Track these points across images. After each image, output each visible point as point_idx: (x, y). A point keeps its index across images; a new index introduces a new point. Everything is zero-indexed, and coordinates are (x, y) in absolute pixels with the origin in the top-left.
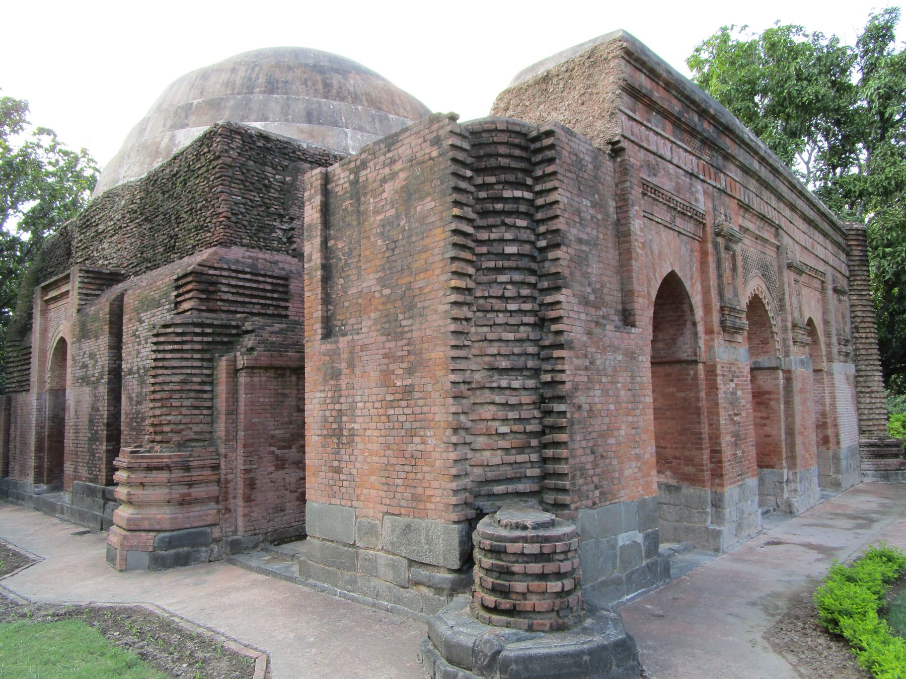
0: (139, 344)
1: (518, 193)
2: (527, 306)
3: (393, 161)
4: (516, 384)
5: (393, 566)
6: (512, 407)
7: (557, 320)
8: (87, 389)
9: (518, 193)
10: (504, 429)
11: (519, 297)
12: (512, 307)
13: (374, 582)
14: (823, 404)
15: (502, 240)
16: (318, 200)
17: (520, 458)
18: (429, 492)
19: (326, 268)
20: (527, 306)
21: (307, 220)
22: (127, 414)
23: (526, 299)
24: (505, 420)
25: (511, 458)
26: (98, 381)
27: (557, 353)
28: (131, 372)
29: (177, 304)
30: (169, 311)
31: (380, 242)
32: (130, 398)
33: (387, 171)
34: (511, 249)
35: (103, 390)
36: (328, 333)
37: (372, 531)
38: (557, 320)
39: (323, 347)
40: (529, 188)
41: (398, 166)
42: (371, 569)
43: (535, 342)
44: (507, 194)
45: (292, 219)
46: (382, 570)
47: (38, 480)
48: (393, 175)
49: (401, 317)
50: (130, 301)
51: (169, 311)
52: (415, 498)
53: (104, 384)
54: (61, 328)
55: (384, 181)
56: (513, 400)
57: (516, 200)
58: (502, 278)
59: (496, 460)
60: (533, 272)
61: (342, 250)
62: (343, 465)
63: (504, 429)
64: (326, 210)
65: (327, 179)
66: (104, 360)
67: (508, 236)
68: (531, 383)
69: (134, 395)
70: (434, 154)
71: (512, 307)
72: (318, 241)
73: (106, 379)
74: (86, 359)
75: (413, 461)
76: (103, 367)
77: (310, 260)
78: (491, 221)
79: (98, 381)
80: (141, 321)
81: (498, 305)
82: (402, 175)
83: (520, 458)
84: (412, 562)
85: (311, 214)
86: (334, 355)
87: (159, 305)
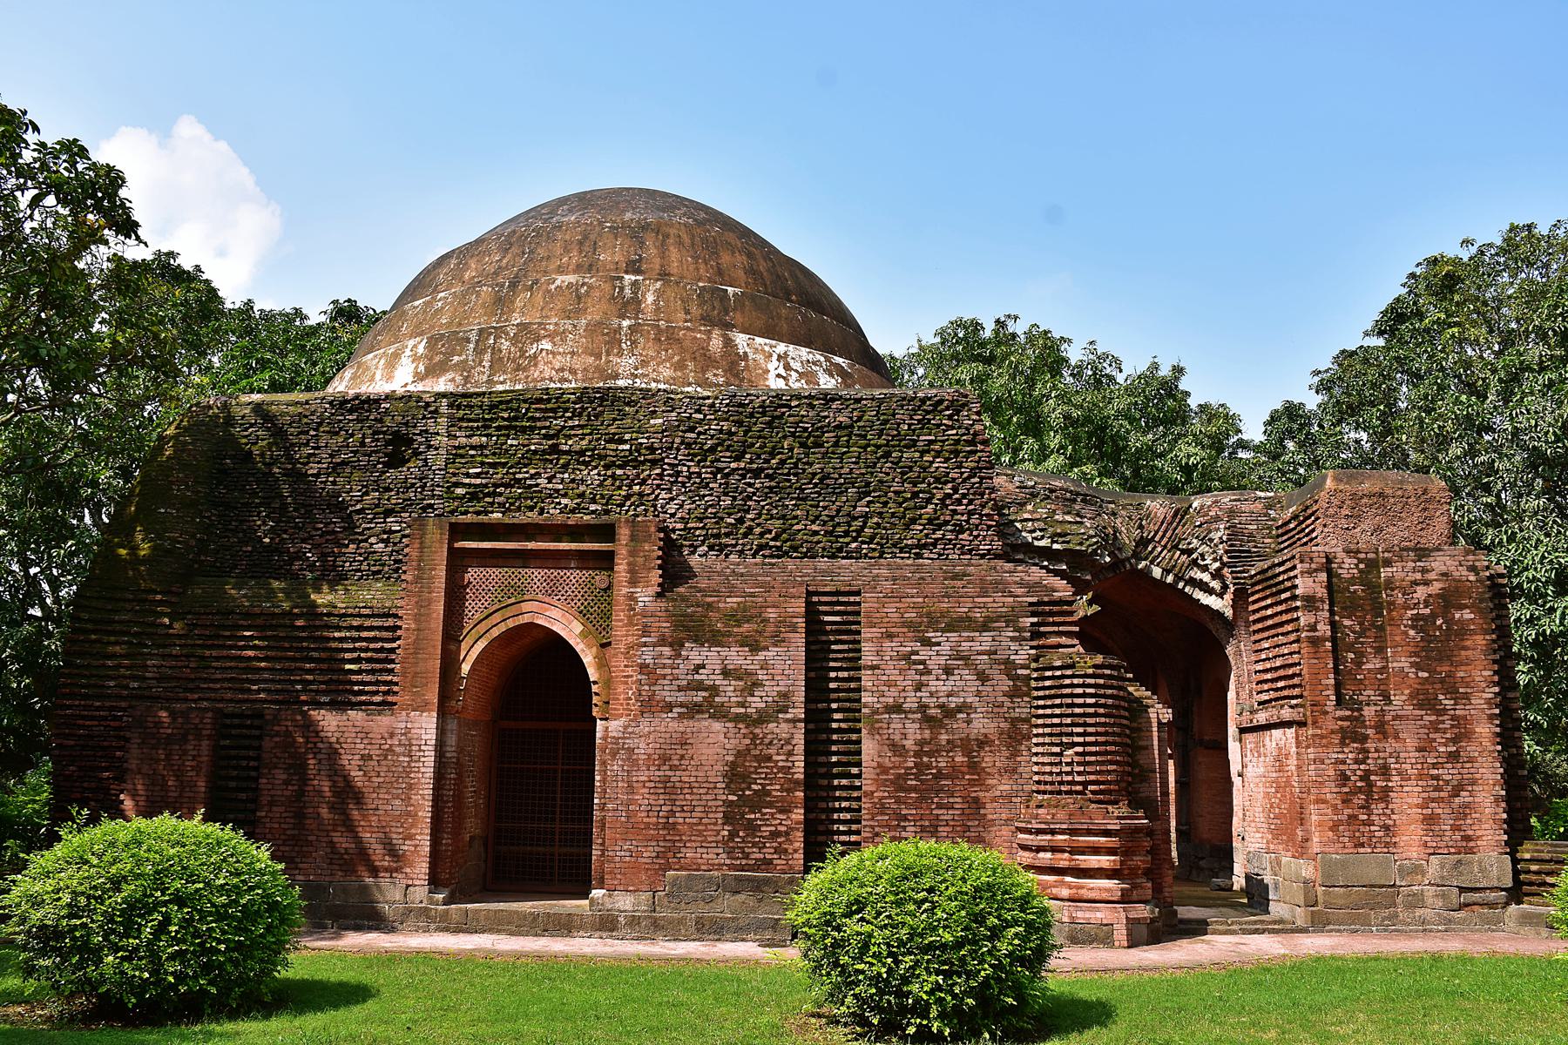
5: (1443, 896)
8: (717, 726)
13: (1419, 912)
16: (1323, 576)
18: (1479, 833)
22: (883, 769)
28: (897, 708)
31: (1412, 633)
33: (1418, 576)
35: (790, 733)
37: (1417, 870)
39: (1339, 713)
41: (1432, 576)
42: (1416, 901)
46: (1430, 901)
47: (435, 882)
48: (1427, 583)
49: (1441, 697)
52: (1467, 838)
53: (794, 721)
61: (1349, 628)
62: (1373, 817)
64: (1330, 587)
69: (909, 743)
70: (1472, 578)
72: (1327, 614)
75: (1464, 812)
76: (785, 695)
84: (1462, 890)
87: (984, 627)
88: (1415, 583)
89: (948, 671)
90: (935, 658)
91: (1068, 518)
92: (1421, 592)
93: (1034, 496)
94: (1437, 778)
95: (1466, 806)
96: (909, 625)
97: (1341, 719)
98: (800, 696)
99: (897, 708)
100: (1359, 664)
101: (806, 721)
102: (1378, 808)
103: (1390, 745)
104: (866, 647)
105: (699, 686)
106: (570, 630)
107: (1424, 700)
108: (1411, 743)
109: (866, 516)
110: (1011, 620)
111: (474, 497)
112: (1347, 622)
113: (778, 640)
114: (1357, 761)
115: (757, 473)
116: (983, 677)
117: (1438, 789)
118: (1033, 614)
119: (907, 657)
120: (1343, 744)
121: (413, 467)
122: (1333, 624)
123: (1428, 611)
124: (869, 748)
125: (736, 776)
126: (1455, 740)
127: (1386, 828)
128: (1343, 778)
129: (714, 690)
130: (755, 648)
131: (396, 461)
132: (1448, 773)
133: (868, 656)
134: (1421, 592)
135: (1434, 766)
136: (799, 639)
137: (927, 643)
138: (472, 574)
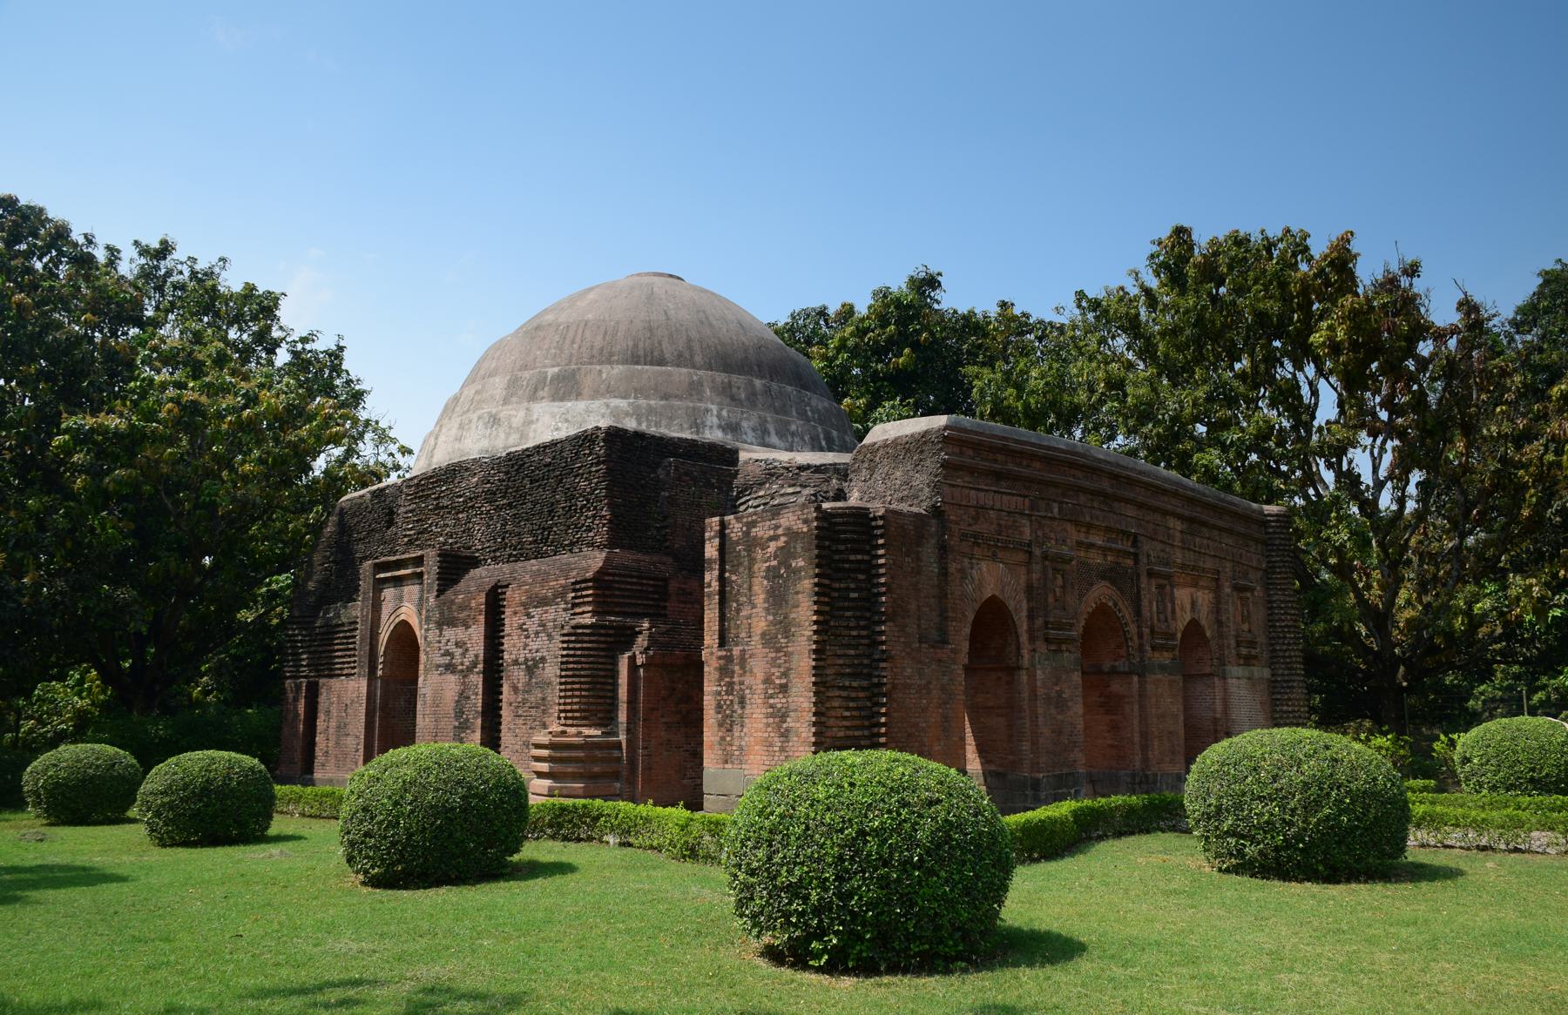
0: (527, 637)
1: (859, 557)
2: (864, 633)
3: (777, 527)
4: (855, 684)
6: (853, 700)
7: (883, 643)
8: (452, 678)
9: (859, 557)
10: (847, 714)
11: (857, 627)
12: (854, 633)
14: (1214, 711)
15: (848, 589)
16: (717, 541)
17: (857, 733)
19: (722, 593)
20: (864, 633)
21: (707, 555)
23: (864, 628)
24: (848, 709)
25: (850, 733)
26: (470, 669)
27: (883, 665)
28: (516, 662)
29: (574, 605)
30: (565, 610)
32: (515, 689)
34: (854, 595)
35: (477, 680)
36: (722, 644)
38: (883, 643)
40: (868, 553)
41: (780, 531)
43: (869, 657)
44: (852, 557)
45: (665, 518)
48: (775, 538)
50: (514, 596)
51: (565, 610)
54: (403, 610)
55: (772, 539)
56: (853, 695)
57: (858, 561)
58: (848, 614)
59: (841, 734)
60: (869, 610)
63: (847, 714)
64: (722, 549)
65: (723, 525)
66: (477, 647)
67: (852, 586)
68: (865, 683)
71: (854, 633)
72: (716, 573)
73: (480, 666)
74: (451, 647)
76: (476, 656)
77: (709, 585)
78: (840, 575)
79: (470, 669)
80: (529, 616)
81: (845, 632)
82: (783, 539)
83: (857, 733)
85: (711, 551)
86: (729, 659)
88: (772, 539)
89: (537, 633)
90: (532, 625)
91: (790, 490)
92: (773, 546)
93: (772, 475)
94: (771, 706)
95: (787, 730)
96: (523, 605)
97: (720, 658)
98: (481, 658)
99: (516, 662)
100: (738, 611)
101: (484, 672)
102: (736, 728)
103: (748, 680)
104: (507, 621)
105: (447, 653)
106: (414, 622)
107: (768, 640)
108: (760, 676)
109: (551, 527)
110: (563, 595)
111: (410, 543)
112: (734, 578)
113: (475, 621)
114: (727, 693)
115: (510, 505)
116: (550, 636)
117: (772, 715)
118: (575, 590)
119: (520, 627)
120: (720, 679)
121: (393, 529)
122: (722, 579)
123: (775, 563)
124: (505, 689)
125: (459, 713)
126: (785, 674)
127: (741, 748)
128: (719, 706)
129: (452, 655)
130: (468, 627)
131: (391, 523)
132: (778, 701)
133: (507, 629)
134: (773, 546)
135: (771, 697)
136: (482, 618)
137: (529, 616)
138: (388, 593)
